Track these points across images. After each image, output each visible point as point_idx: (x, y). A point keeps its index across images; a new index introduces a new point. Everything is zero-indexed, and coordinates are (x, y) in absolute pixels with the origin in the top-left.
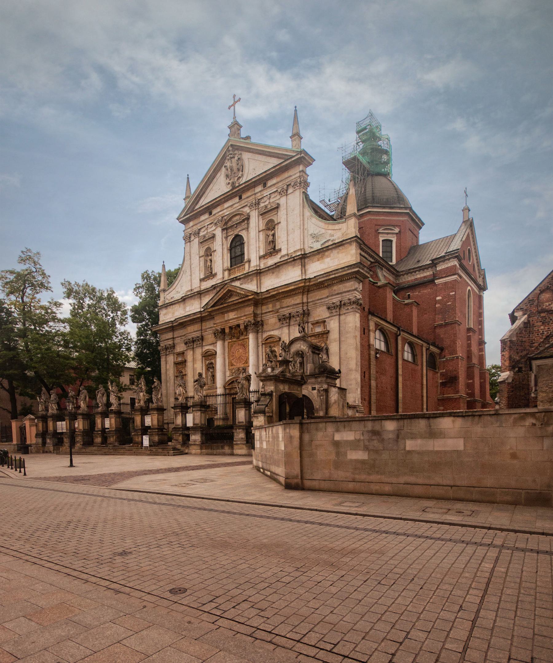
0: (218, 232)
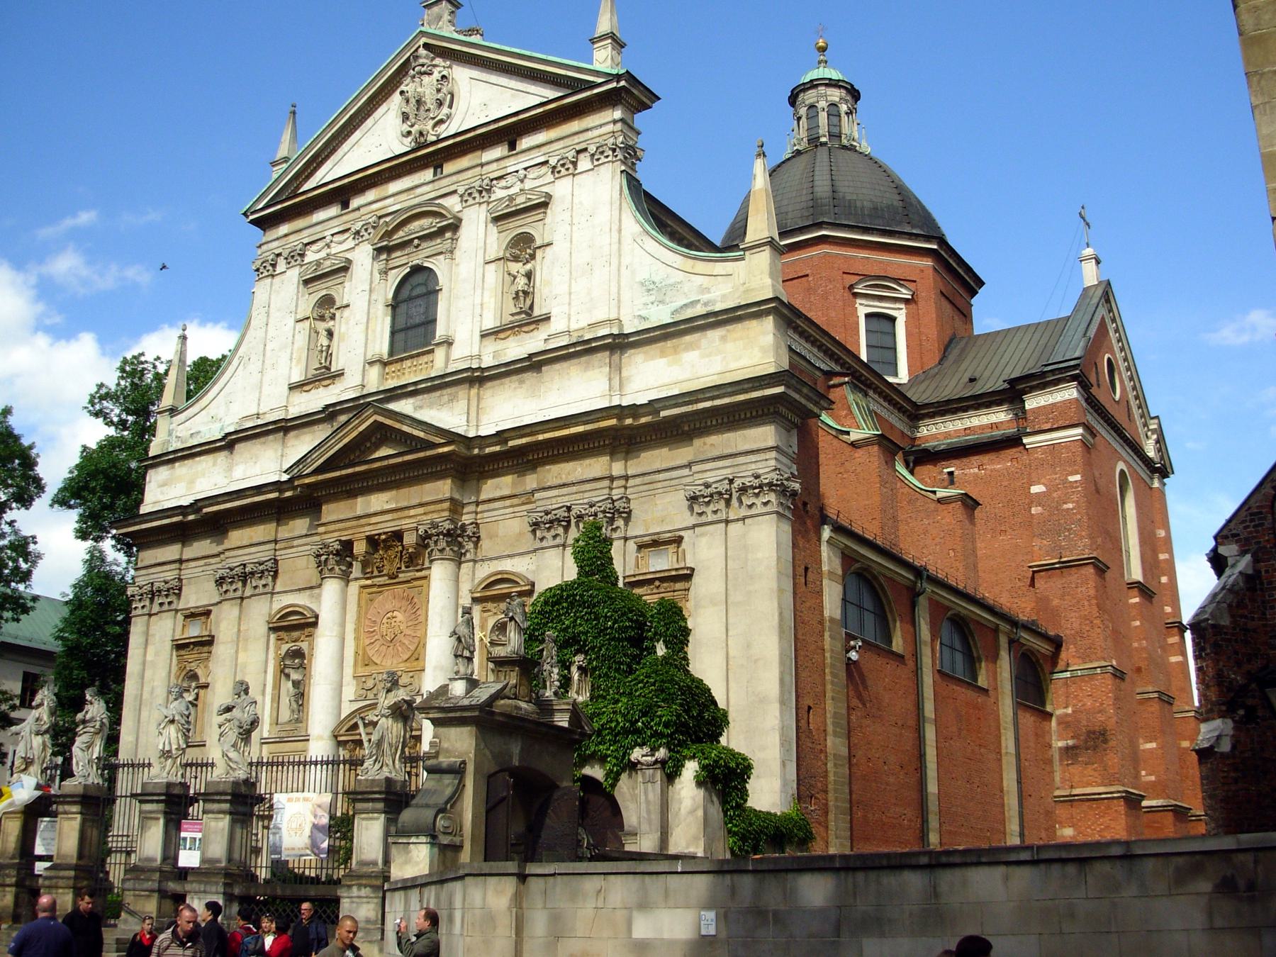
0: (362, 257)
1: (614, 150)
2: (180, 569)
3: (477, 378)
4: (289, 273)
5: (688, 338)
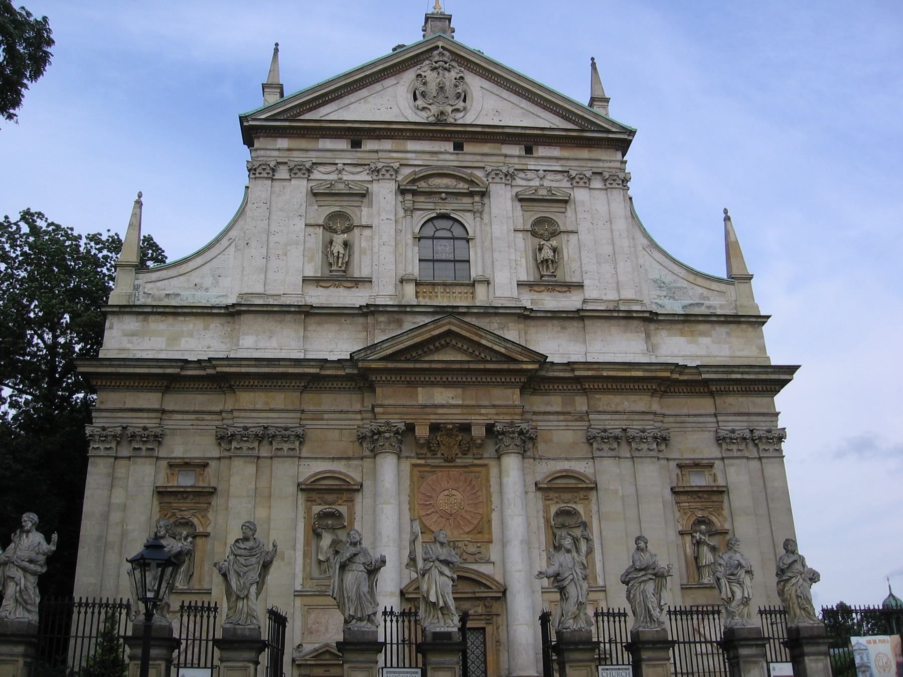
1: (623, 181)
2: (161, 419)
3: (525, 316)
4: (293, 181)
5: (702, 327)
